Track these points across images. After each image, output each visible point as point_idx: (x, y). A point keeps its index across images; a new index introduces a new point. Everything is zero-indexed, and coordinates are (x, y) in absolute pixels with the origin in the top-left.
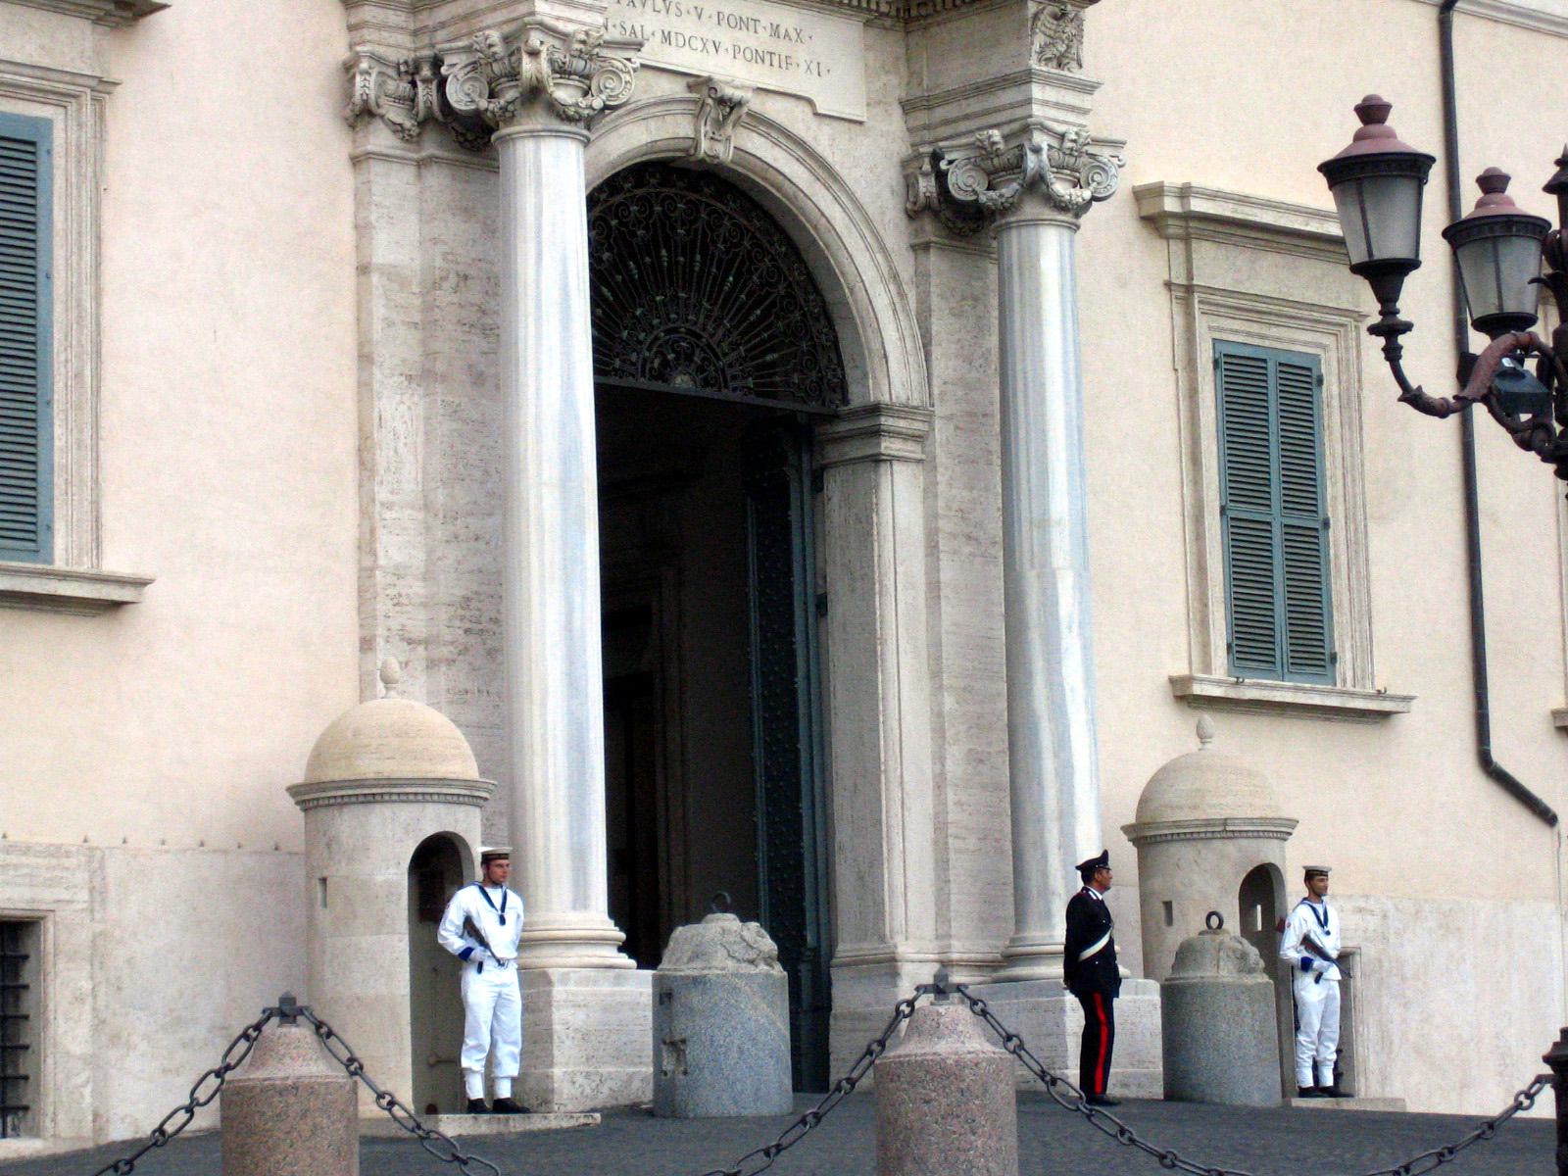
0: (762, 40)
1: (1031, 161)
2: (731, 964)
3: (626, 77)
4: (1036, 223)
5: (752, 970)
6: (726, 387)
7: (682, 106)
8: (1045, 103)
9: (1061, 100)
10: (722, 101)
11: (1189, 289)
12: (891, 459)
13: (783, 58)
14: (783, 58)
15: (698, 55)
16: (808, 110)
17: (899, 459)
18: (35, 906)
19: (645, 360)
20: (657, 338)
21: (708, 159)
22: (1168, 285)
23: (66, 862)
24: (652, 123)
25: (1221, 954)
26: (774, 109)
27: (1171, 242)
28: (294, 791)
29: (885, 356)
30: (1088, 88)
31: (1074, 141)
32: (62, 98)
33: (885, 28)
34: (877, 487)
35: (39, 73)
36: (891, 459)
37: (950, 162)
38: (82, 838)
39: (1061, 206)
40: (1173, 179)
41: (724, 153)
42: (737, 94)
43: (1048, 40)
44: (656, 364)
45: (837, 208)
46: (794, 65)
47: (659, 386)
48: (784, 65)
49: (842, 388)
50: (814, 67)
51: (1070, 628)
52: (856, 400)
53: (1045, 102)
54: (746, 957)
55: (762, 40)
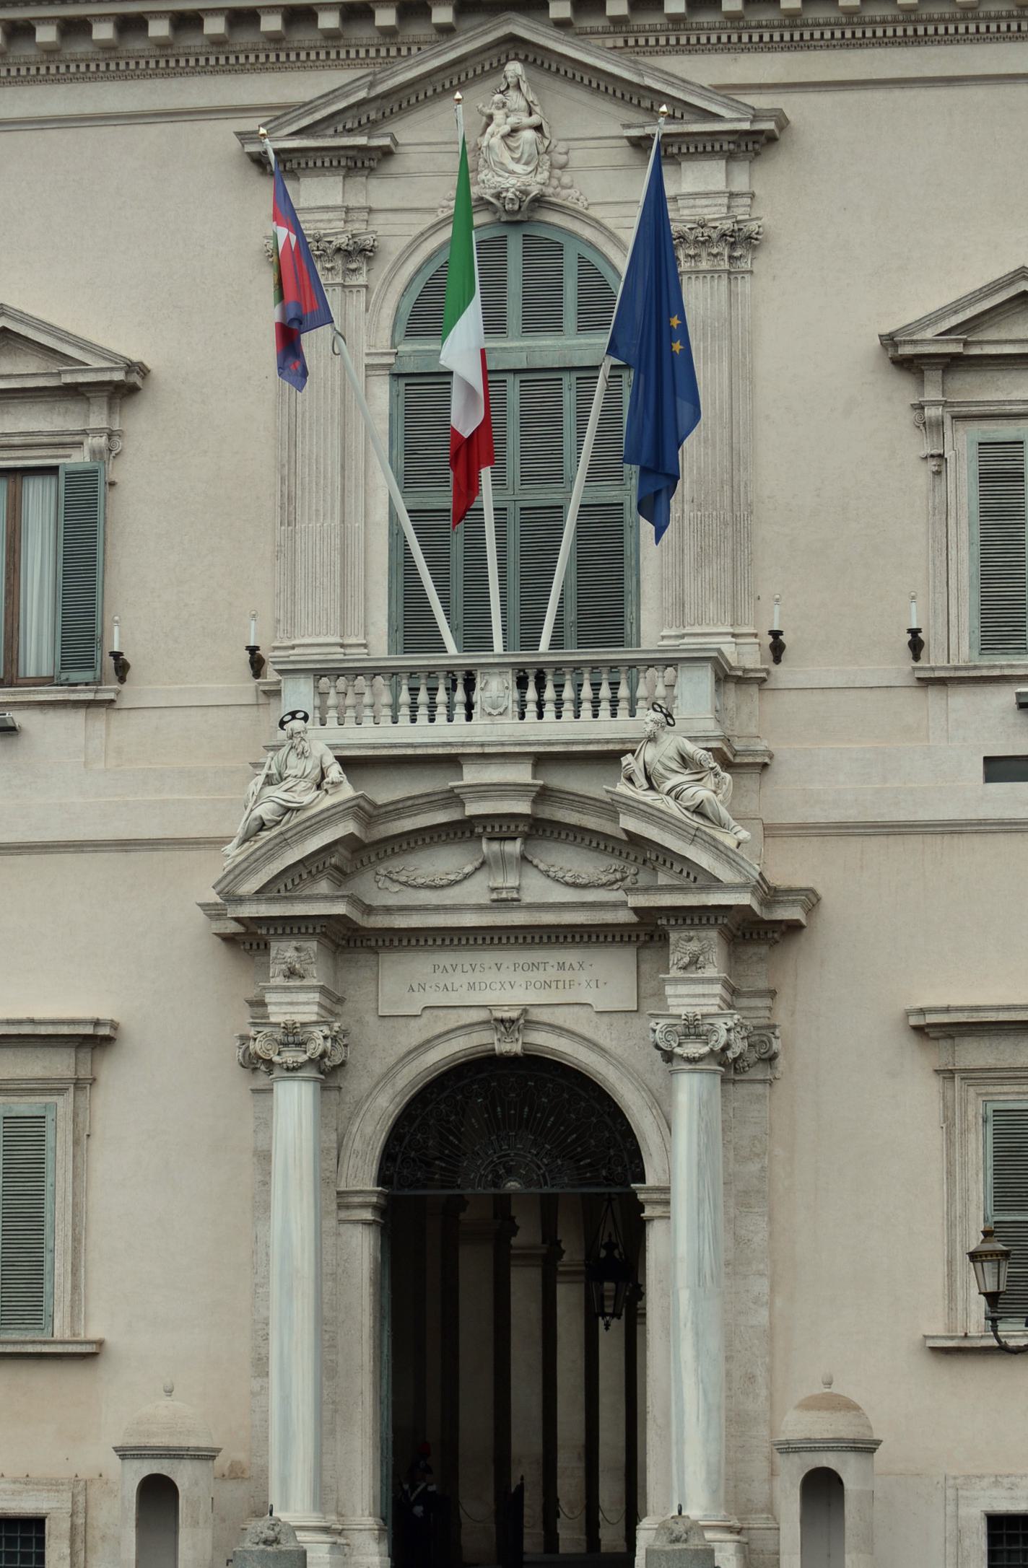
0: (552, 973)
2: (249, 1544)
3: (318, 1042)
5: (256, 1548)
10: (502, 1021)
12: (651, 1219)
13: (567, 983)
14: (567, 983)
18: (38, 1511)
20: (492, 1162)
26: (558, 1017)
31: (685, 1020)
32: (61, 1091)
35: (40, 1082)
36: (651, 1219)
38: (74, 1475)
41: (517, 1048)
42: (506, 1015)
43: (683, 955)
45: (611, 1067)
46: (576, 984)
47: (492, 1190)
48: (567, 986)
50: (593, 984)
51: (685, 1325)
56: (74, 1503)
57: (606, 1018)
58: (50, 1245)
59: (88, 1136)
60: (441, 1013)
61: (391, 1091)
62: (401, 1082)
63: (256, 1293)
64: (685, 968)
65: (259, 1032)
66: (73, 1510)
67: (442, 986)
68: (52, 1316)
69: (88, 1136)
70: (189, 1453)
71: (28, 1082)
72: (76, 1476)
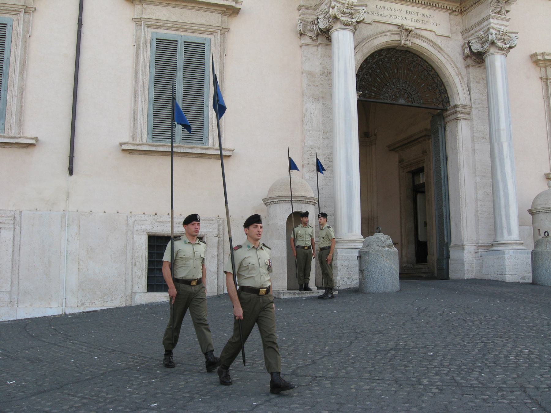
1: (490, 37)
2: (377, 248)
3: (362, 13)
4: (493, 54)
5: (383, 249)
6: (415, 102)
7: (397, 32)
8: (495, 24)
9: (499, 23)
10: (406, 30)
11: (547, 79)
13: (426, 21)
15: (401, 20)
16: (433, 34)
17: (463, 119)
19: (390, 96)
21: (405, 46)
22: (541, 78)
23: (212, 222)
24: (387, 37)
25: (548, 243)
26: (424, 33)
27: (541, 68)
28: (264, 200)
29: (458, 94)
30: (508, 20)
31: (503, 31)
32: (213, 33)
33: (456, 15)
34: (457, 126)
35: (204, 26)
37: (472, 43)
39: (501, 49)
40: (540, 51)
41: (409, 44)
42: (410, 28)
43: (495, 8)
44: (394, 97)
45: (443, 57)
48: (426, 23)
49: (448, 102)
50: (435, 24)
51: (507, 157)
52: (452, 104)
53: (495, 23)
54: (382, 245)
55: (420, 17)
56: (218, 230)
57: (439, 38)
58: (207, 104)
59: (225, 55)
60: (380, 25)
61: (361, 53)
62: (365, 50)
63: (306, 134)
64: (495, 13)
65: (335, 5)
66: (218, 233)
67: (380, 14)
68: (208, 137)
69: (225, 55)
70: (314, 201)
71: (199, 26)
72: (219, 216)
